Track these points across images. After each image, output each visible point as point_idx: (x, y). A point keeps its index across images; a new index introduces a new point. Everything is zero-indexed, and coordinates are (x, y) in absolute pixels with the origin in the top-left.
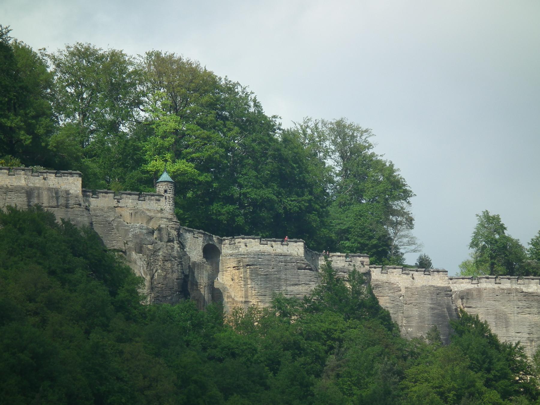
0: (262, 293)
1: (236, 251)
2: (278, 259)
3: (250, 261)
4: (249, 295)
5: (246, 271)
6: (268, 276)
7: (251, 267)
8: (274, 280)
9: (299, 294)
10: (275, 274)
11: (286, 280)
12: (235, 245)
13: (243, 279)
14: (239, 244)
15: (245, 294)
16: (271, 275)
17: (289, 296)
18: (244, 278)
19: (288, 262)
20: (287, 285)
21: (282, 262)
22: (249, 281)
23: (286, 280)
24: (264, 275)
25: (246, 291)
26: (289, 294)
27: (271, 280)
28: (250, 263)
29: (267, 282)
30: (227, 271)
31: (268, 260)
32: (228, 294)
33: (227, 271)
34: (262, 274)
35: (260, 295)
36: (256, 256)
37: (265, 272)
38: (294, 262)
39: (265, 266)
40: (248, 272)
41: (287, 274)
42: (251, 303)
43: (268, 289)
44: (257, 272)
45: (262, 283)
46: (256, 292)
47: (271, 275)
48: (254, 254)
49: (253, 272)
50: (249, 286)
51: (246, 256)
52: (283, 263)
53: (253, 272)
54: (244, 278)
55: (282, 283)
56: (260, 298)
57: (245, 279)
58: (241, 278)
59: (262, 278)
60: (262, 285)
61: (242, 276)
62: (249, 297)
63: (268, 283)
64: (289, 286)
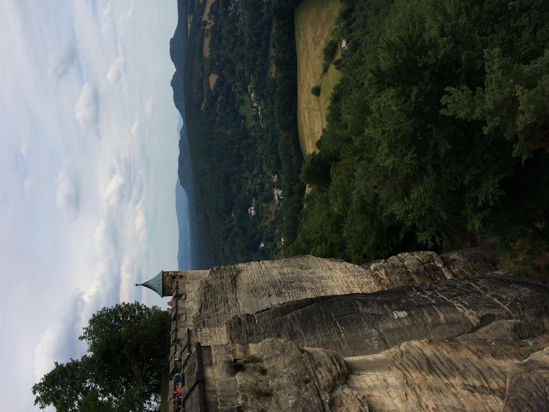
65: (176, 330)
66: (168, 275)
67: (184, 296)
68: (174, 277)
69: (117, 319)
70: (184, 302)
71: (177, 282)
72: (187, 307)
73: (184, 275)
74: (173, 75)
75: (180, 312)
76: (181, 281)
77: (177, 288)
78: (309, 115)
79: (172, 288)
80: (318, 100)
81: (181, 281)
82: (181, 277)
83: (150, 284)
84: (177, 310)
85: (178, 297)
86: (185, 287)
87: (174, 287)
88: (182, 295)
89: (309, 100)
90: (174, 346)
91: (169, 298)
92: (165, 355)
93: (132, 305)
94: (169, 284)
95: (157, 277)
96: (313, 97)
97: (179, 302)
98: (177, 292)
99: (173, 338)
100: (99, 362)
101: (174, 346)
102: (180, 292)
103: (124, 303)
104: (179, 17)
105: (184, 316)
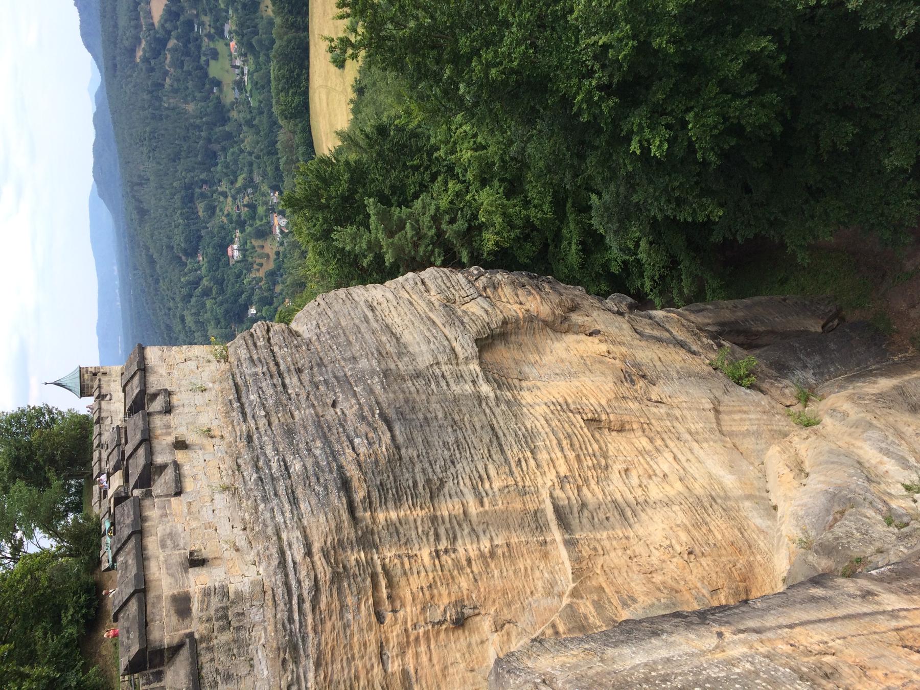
0: (486, 439)
1: (255, 615)
2: (270, 402)
3: (324, 503)
4: (518, 505)
5: (394, 529)
6: (391, 413)
7: (359, 495)
8: (404, 392)
9: (429, 319)
10: (371, 391)
11: (382, 355)
12: (207, 638)
13: (444, 544)
14: (195, 606)
15: (522, 526)
16: (378, 403)
17: (454, 344)
18: (437, 537)
19: (273, 369)
20: (403, 350)
21: (284, 386)
22: (447, 508)
23: (382, 355)
24: (391, 429)
25: (504, 521)
26: (446, 343)
27: (407, 401)
28: (338, 500)
29: (426, 419)
30: (405, 673)
31: (289, 433)
32: (561, 628)
33: (405, 673)
34: (386, 438)
35: (502, 451)
36: (281, 488)
37: (375, 429)
38: (272, 351)
39: (333, 438)
40: (393, 515)
41: (348, 355)
42: (558, 493)
43: (457, 418)
44: (383, 462)
45: (435, 440)
46: (492, 471)
47: (378, 403)
48: (265, 500)
49: (390, 483)
50: (473, 509)
51: (292, 536)
52: (292, 381)
53: (390, 483)
54: (437, 537)
55: (403, 366)
56: (513, 453)
57: (442, 531)
58: (444, 558)
59: (411, 440)
60: (451, 440)
61: (425, 554)
62: (531, 507)
63: (429, 415)
64: (405, 348)
65: (100, 434)
66: (87, 371)
67: (108, 397)
68: (95, 374)
69: (21, 425)
70: (109, 403)
71: (100, 380)
72: (112, 408)
73: (108, 371)
74: (78, 32)
75: (103, 415)
76: (104, 379)
77: (99, 387)
78: (328, 99)
79: (92, 388)
80: (342, 76)
81: (104, 379)
82: (104, 374)
83: (62, 382)
84: (100, 412)
85: (101, 397)
86: (109, 385)
87: (95, 386)
88: (106, 395)
89: (328, 72)
90: (97, 452)
91: (90, 401)
92: (87, 462)
93: (40, 409)
94: (89, 382)
95: (73, 374)
96: (333, 69)
97: (103, 403)
98: (100, 392)
99: (96, 443)
100: (9, 469)
101: (97, 452)
102: (104, 392)
103: (29, 406)
104: (99, 320)
105: (109, 419)
